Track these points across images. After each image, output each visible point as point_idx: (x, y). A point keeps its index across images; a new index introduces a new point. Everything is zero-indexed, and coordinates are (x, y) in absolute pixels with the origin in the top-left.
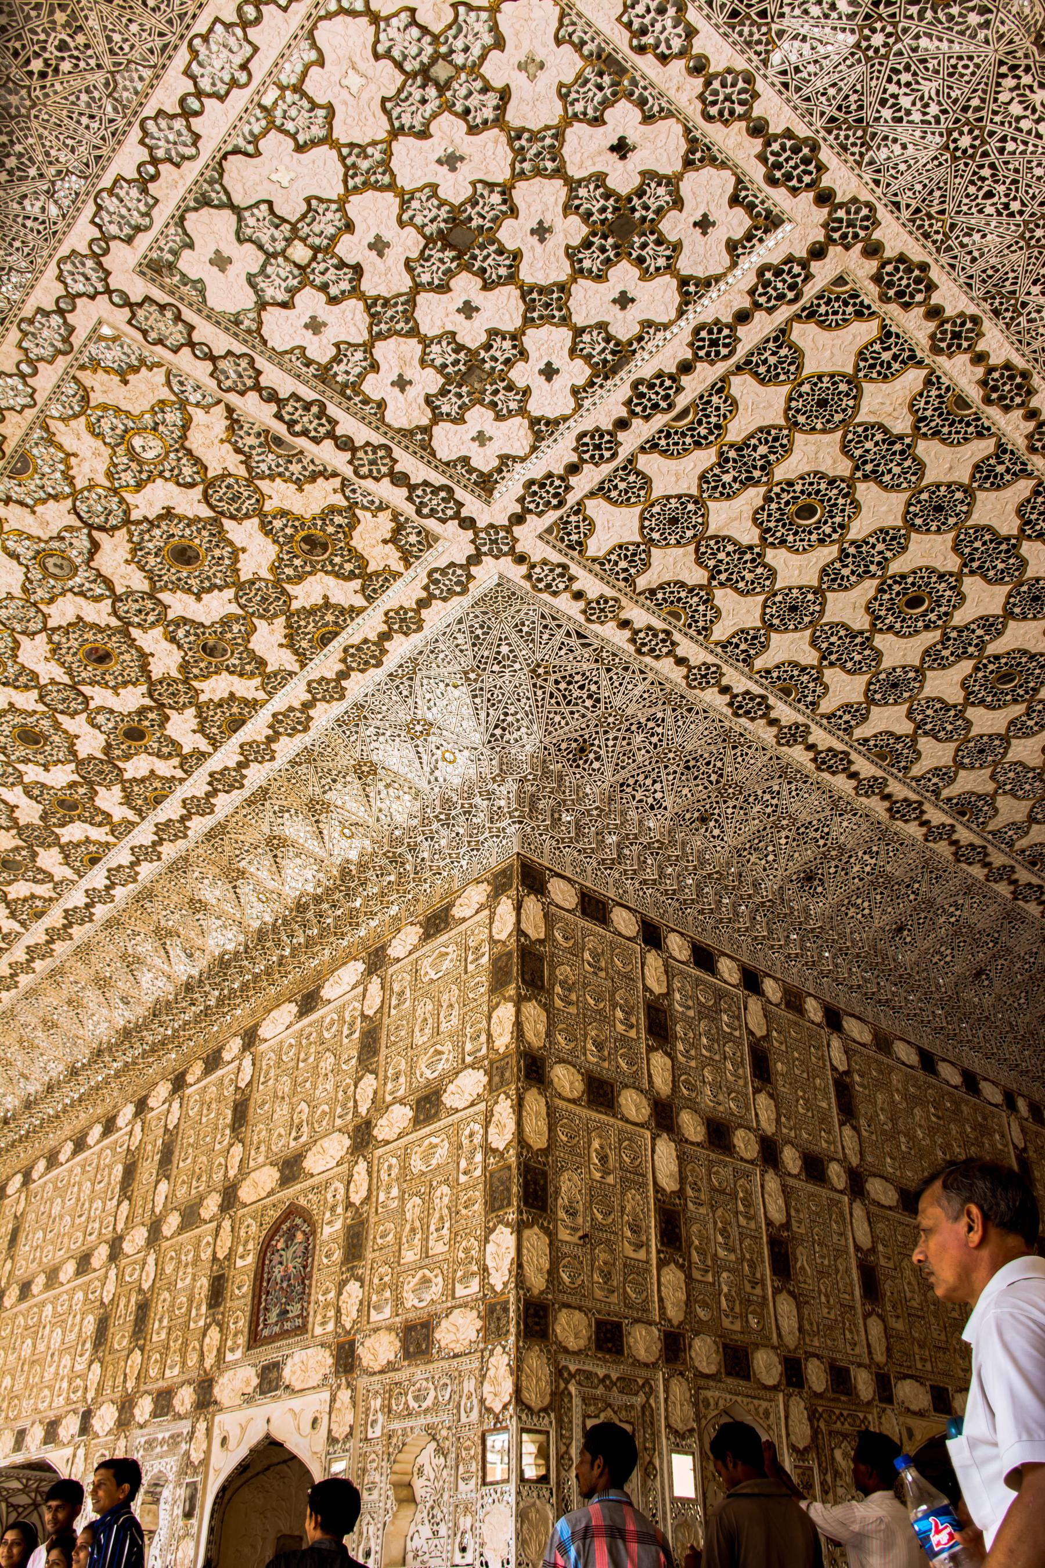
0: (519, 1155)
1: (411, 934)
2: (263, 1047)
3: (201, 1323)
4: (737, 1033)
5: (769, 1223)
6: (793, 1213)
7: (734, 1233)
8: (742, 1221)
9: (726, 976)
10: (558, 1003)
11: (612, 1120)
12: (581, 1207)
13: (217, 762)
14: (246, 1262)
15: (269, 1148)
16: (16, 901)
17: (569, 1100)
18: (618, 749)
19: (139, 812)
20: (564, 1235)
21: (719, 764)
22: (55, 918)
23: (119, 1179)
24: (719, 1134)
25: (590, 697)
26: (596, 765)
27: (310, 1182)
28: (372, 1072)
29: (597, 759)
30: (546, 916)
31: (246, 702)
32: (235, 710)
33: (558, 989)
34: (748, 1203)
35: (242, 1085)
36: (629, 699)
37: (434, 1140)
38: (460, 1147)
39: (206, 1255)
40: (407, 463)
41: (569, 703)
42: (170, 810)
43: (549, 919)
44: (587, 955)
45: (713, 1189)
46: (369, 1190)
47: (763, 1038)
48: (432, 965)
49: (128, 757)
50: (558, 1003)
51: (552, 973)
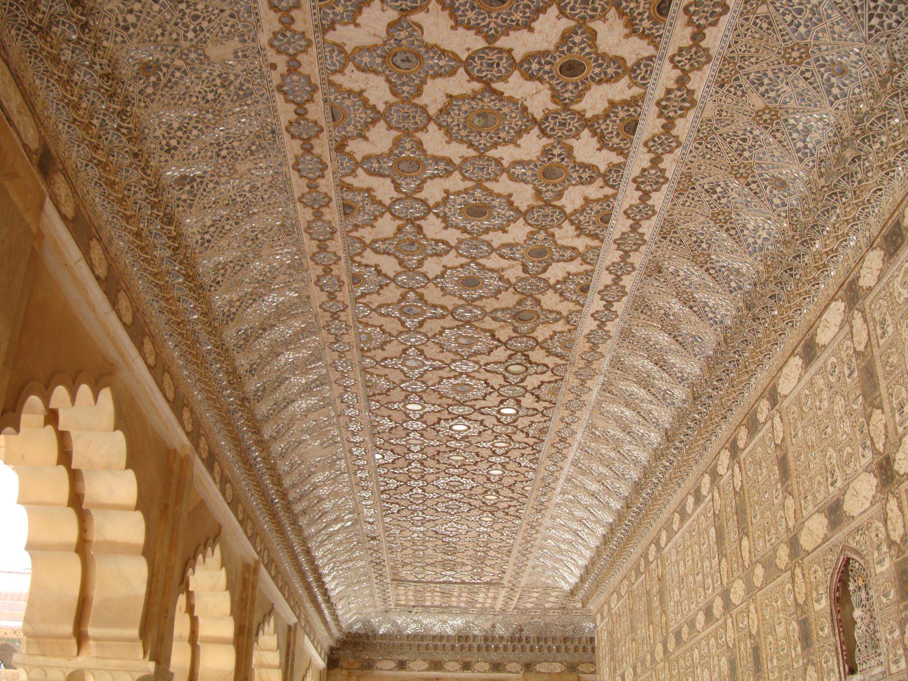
1: (875, 258)
2: (786, 403)
3: (801, 663)
13: (633, 170)
14: (823, 605)
15: (815, 497)
16: (545, 341)
19: (595, 236)
22: (582, 346)
23: (714, 540)
27: (854, 525)
28: (878, 408)
31: (625, 103)
32: (622, 114)
35: (778, 442)
39: (790, 602)
42: (620, 225)
49: (560, 195)
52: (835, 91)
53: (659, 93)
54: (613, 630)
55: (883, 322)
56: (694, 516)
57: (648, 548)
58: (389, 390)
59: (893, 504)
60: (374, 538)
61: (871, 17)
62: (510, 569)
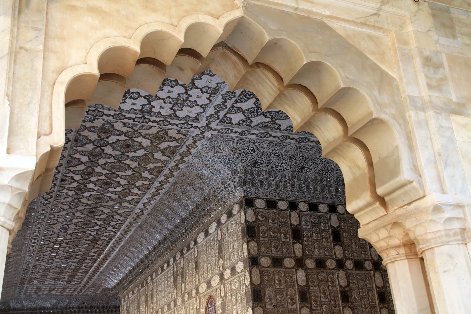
0: (251, 287)
2: (199, 245)
4: (327, 228)
5: (340, 286)
6: (351, 281)
7: (327, 292)
8: (330, 288)
9: (322, 210)
10: (261, 239)
11: (282, 269)
12: (273, 297)
17: (267, 267)
18: (266, 160)
20: (268, 306)
21: (301, 154)
22: (133, 215)
24: (320, 263)
25: (252, 151)
26: (261, 166)
29: (261, 164)
30: (255, 213)
33: (261, 234)
34: (333, 282)
35: (196, 256)
36: (264, 147)
37: (236, 280)
38: (241, 283)
39: (195, 307)
40: (172, 121)
41: (246, 154)
42: (152, 190)
43: (256, 214)
44: (270, 220)
45: (319, 281)
46: (225, 293)
47: (337, 227)
48: (231, 227)
50: (261, 239)
51: (258, 230)
52: (218, 175)
53: (170, 166)
54: (129, 307)
55: (225, 235)
56: (167, 271)
57: (147, 278)
58: (56, 223)
59: (222, 286)
60: (27, 270)
61: (228, 164)
62: (85, 280)
